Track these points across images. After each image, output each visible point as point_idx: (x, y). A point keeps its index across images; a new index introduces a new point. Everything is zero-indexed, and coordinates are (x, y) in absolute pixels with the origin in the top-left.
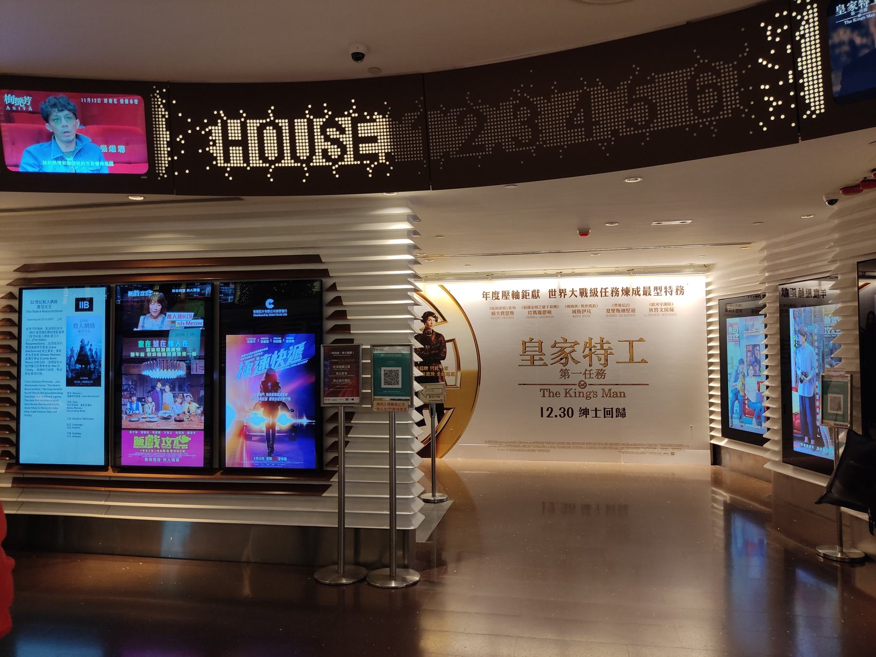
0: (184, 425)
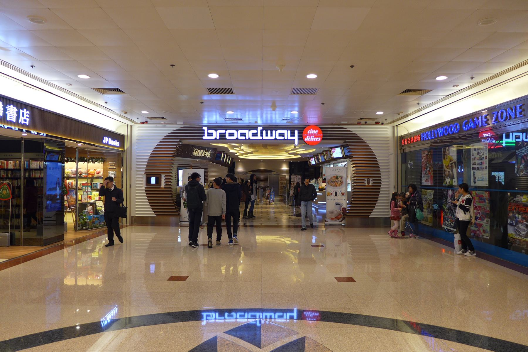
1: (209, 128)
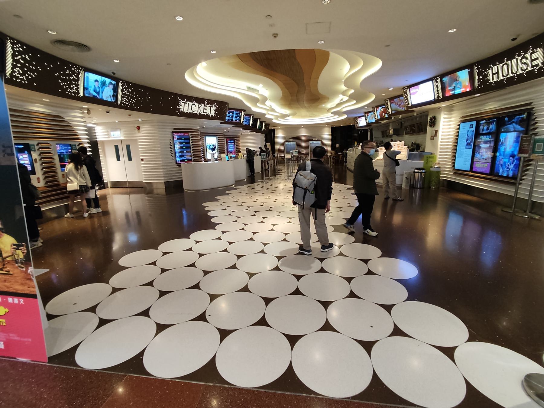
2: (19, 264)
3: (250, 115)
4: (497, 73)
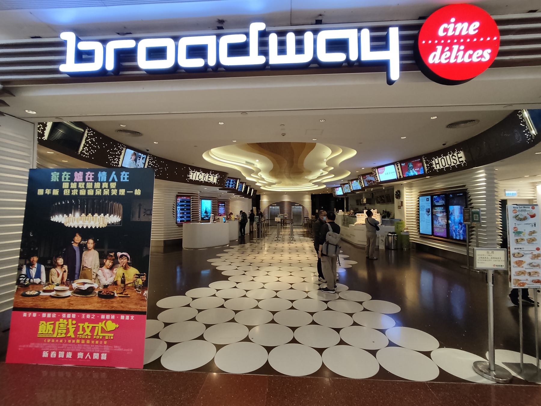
0: (115, 304)
1: (82, 33)
2: (137, 289)
3: (243, 183)
4: (439, 163)
